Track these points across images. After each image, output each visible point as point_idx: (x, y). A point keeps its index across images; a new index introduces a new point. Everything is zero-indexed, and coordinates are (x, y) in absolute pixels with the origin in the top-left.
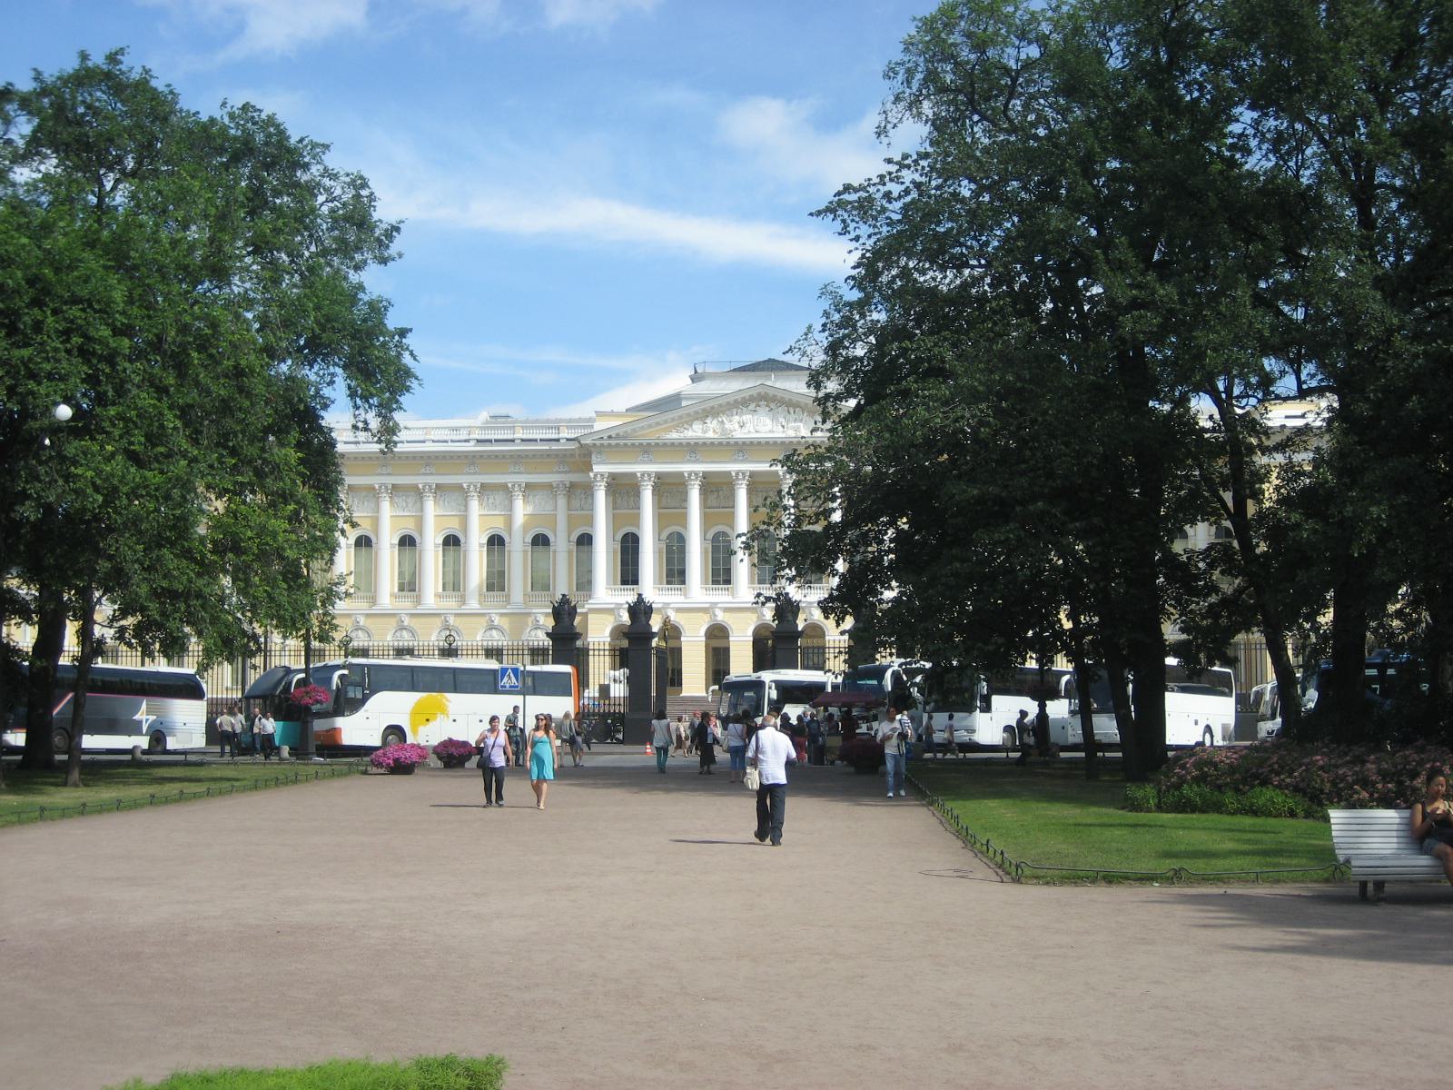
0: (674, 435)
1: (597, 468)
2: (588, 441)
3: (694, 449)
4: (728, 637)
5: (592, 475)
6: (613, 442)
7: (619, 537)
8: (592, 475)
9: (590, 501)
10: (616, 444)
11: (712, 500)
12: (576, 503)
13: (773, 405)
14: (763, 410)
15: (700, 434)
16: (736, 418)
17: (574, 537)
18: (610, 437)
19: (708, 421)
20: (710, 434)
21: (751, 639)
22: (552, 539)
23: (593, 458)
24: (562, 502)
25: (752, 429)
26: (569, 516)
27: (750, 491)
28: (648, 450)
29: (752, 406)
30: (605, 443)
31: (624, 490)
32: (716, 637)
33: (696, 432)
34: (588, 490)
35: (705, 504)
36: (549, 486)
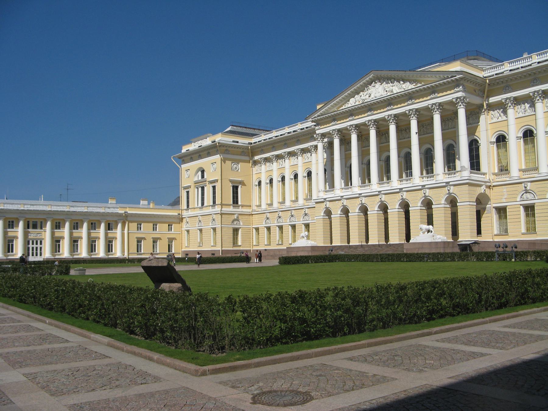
0: (344, 107)
1: (317, 132)
3: (352, 113)
18: (319, 116)
20: (357, 103)
29: (373, 84)
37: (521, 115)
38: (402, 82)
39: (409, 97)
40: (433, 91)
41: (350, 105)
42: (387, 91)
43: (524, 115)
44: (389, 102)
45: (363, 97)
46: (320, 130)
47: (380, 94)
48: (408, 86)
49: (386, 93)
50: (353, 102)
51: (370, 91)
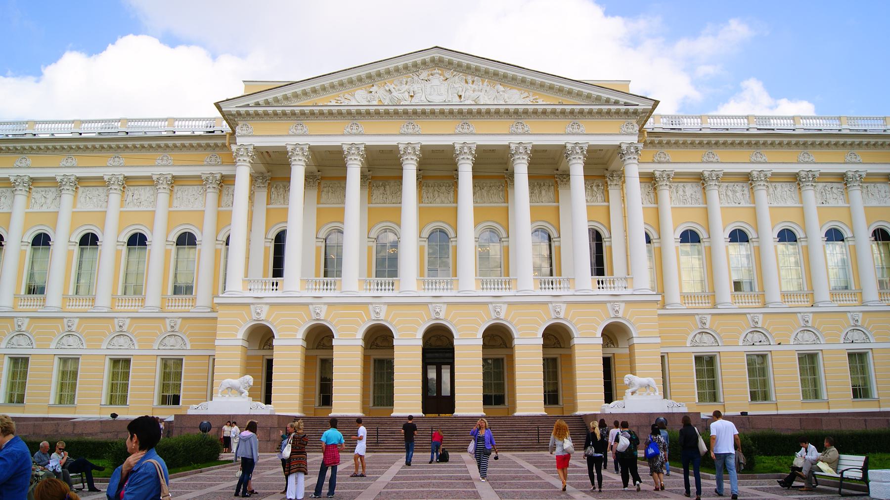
1: (239, 141)
2: (232, 108)
4: (392, 347)
5: (234, 148)
6: (260, 110)
8: (234, 148)
11: (377, 193)
13: (448, 74)
14: (436, 81)
16: (405, 88)
18: (258, 104)
19: (374, 89)
21: (420, 343)
24: (211, 196)
25: (423, 98)
29: (424, 74)
31: (272, 170)
32: (378, 347)
33: (359, 98)
36: (198, 180)
38: (501, 88)
42: (460, 96)
43: (682, 205)
46: (252, 138)
49: (456, 100)
51: (416, 87)
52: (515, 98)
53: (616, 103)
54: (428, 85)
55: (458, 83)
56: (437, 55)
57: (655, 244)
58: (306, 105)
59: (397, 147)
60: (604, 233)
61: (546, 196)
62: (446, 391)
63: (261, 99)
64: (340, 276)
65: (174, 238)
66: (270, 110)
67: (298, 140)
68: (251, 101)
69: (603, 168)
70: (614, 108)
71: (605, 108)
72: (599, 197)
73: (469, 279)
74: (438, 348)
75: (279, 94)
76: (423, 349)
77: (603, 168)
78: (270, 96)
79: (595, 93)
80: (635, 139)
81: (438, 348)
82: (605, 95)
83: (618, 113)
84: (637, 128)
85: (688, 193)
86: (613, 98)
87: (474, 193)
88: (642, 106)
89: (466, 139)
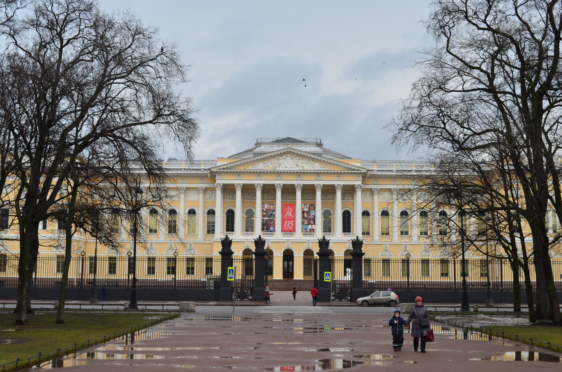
1: (218, 182)
2: (215, 170)
3: (259, 173)
7: (226, 211)
8: (215, 184)
9: (213, 196)
10: (226, 171)
11: (266, 195)
12: (207, 196)
13: (293, 156)
14: (289, 159)
15: (262, 168)
16: (277, 162)
17: (206, 211)
18: (224, 168)
19: (266, 162)
20: (266, 168)
22: (197, 212)
23: (216, 177)
24: (201, 196)
26: (204, 202)
27: (283, 192)
28: (239, 173)
29: (284, 157)
30: (222, 171)
31: (228, 190)
33: (261, 166)
34: (213, 190)
35: (263, 198)
36: (196, 189)
37: (381, 200)
38: (312, 162)
39: (318, 174)
40: (339, 174)
41: (259, 168)
44: (299, 174)
45: (274, 165)
47: (290, 166)
48: (317, 167)
50: (261, 166)
51: (281, 162)
52: (317, 167)
53: (354, 169)
54: (286, 161)
55: (297, 160)
56: (289, 150)
57: (371, 217)
58: (242, 169)
59: (274, 185)
60: (351, 213)
61: (330, 197)
62: (290, 271)
63: (225, 167)
64: (253, 231)
65: (187, 212)
66: (229, 171)
67: (238, 182)
68: (222, 168)
69: (349, 191)
70: (353, 172)
71: (349, 172)
72: (351, 198)
73: (299, 235)
74: (288, 256)
75: (232, 165)
76: (284, 256)
77: (349, 191)
78: (228, 166)
79: (346, 166)
80: (360, 183)
81: (288, 256)
82: (350, 167)
83: (354, 173)
84: (361, 178)
85: (386, 196)
86: (353, 168)
87: (302, 196)
88: (363, 171)
89: (299, 182)
